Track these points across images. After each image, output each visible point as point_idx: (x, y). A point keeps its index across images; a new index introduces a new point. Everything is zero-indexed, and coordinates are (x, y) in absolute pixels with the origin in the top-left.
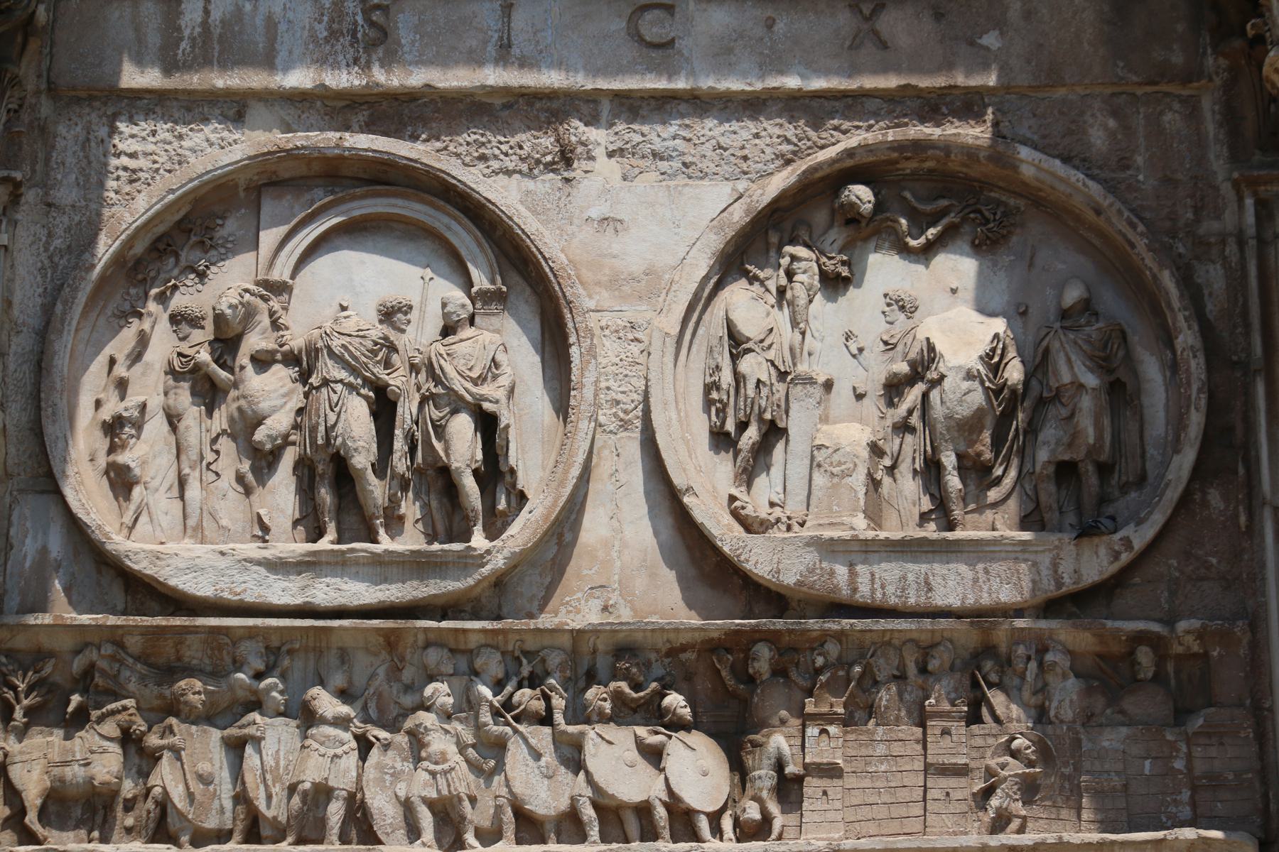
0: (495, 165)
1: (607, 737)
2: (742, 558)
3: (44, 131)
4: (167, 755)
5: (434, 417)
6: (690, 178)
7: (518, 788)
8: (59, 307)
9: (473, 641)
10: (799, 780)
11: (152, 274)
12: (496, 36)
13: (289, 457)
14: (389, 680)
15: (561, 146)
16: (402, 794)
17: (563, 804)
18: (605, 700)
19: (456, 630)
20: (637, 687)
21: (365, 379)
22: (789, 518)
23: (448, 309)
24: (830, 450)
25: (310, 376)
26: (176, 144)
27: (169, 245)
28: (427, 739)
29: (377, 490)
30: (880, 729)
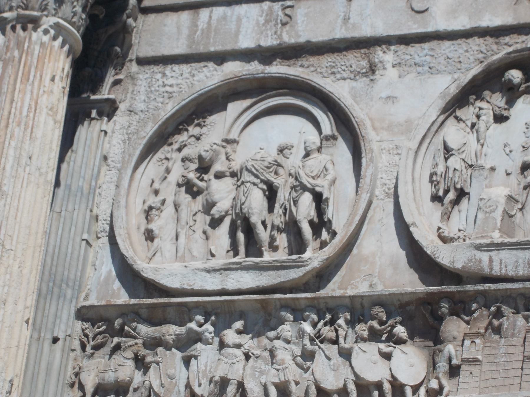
0: (338, 76)
1: (363, 349)
2: (436, 256)
3: (132, 78)
4: (154, 365)
6: (432, 74)
7: (318, 376)
9: (303, 304)
10: (458, 367)
11: (176, 140)
12: (343, 14)
13: (227, 221)
15: (370, 64)
16: (263, 381)
17: (341, 385)
18: (365, 330)
22: (465, 236)
24: (487, 200)
26: (191, 79)
28: (277, 353)
29: (263, 235)
30: (503, 340)
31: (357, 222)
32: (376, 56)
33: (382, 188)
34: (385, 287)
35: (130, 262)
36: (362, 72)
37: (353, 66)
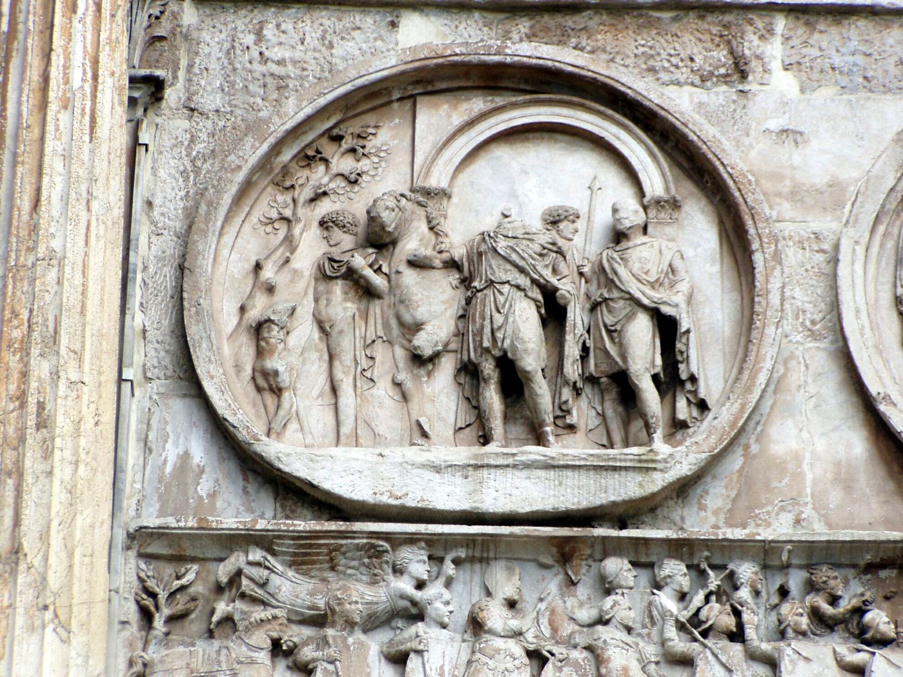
0: (665, 77)
5: (608, 322)
6: (870, 90)
8: (203, 208)
11: (300, 182)
14: (562, 595)
15: (736, 59)
18: (802, 615)
19: (637, 539)
20: (834, 600)
21: (534, 281)
25: (471, 281)
27: (318, 152)
32: (746, 44)
33: (797, 318)
34: (830, 526)
35: (242, 435)
36: (716, 73)
37: (696, 58)
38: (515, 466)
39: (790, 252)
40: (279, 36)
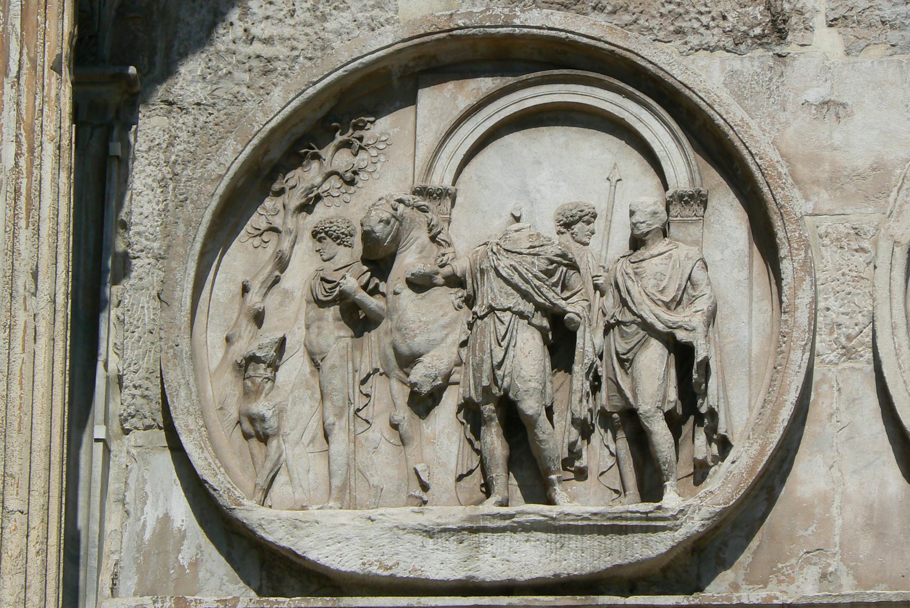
0: (694, 40)
5: (619, 349)
11: (291, 183)
13: (451, 400)
21: (539, 307)
23: (637, 218)
31: (786, 424)
33: (831, 333)
34: (860, 581)
35: (224, 500)
36: (752, 34)
37: (730, 19)
38: (513, 530)
39: (827, 253)
40: (266, 9)
